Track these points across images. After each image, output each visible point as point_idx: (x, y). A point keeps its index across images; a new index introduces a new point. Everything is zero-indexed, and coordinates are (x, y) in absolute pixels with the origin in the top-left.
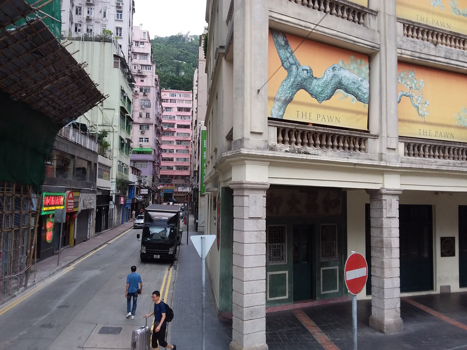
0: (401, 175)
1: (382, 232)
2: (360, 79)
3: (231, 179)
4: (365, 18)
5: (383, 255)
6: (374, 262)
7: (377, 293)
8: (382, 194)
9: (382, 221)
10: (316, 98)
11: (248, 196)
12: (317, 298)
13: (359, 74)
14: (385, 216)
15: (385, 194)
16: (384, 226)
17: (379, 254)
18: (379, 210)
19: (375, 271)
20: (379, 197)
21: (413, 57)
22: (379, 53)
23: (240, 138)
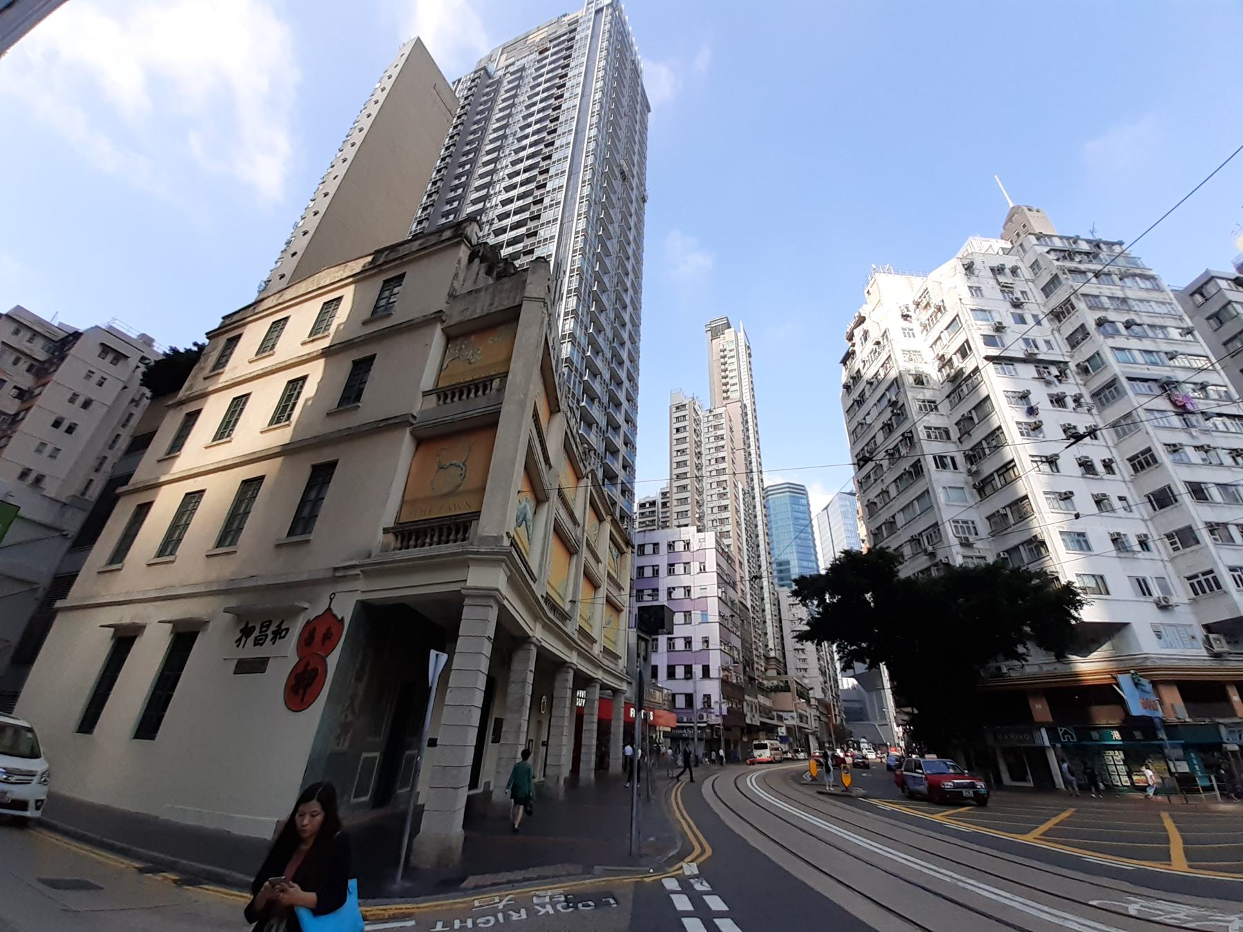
0: (543, 627)
11: (492, 607)
20: (526, 646)
23: (495, 535)
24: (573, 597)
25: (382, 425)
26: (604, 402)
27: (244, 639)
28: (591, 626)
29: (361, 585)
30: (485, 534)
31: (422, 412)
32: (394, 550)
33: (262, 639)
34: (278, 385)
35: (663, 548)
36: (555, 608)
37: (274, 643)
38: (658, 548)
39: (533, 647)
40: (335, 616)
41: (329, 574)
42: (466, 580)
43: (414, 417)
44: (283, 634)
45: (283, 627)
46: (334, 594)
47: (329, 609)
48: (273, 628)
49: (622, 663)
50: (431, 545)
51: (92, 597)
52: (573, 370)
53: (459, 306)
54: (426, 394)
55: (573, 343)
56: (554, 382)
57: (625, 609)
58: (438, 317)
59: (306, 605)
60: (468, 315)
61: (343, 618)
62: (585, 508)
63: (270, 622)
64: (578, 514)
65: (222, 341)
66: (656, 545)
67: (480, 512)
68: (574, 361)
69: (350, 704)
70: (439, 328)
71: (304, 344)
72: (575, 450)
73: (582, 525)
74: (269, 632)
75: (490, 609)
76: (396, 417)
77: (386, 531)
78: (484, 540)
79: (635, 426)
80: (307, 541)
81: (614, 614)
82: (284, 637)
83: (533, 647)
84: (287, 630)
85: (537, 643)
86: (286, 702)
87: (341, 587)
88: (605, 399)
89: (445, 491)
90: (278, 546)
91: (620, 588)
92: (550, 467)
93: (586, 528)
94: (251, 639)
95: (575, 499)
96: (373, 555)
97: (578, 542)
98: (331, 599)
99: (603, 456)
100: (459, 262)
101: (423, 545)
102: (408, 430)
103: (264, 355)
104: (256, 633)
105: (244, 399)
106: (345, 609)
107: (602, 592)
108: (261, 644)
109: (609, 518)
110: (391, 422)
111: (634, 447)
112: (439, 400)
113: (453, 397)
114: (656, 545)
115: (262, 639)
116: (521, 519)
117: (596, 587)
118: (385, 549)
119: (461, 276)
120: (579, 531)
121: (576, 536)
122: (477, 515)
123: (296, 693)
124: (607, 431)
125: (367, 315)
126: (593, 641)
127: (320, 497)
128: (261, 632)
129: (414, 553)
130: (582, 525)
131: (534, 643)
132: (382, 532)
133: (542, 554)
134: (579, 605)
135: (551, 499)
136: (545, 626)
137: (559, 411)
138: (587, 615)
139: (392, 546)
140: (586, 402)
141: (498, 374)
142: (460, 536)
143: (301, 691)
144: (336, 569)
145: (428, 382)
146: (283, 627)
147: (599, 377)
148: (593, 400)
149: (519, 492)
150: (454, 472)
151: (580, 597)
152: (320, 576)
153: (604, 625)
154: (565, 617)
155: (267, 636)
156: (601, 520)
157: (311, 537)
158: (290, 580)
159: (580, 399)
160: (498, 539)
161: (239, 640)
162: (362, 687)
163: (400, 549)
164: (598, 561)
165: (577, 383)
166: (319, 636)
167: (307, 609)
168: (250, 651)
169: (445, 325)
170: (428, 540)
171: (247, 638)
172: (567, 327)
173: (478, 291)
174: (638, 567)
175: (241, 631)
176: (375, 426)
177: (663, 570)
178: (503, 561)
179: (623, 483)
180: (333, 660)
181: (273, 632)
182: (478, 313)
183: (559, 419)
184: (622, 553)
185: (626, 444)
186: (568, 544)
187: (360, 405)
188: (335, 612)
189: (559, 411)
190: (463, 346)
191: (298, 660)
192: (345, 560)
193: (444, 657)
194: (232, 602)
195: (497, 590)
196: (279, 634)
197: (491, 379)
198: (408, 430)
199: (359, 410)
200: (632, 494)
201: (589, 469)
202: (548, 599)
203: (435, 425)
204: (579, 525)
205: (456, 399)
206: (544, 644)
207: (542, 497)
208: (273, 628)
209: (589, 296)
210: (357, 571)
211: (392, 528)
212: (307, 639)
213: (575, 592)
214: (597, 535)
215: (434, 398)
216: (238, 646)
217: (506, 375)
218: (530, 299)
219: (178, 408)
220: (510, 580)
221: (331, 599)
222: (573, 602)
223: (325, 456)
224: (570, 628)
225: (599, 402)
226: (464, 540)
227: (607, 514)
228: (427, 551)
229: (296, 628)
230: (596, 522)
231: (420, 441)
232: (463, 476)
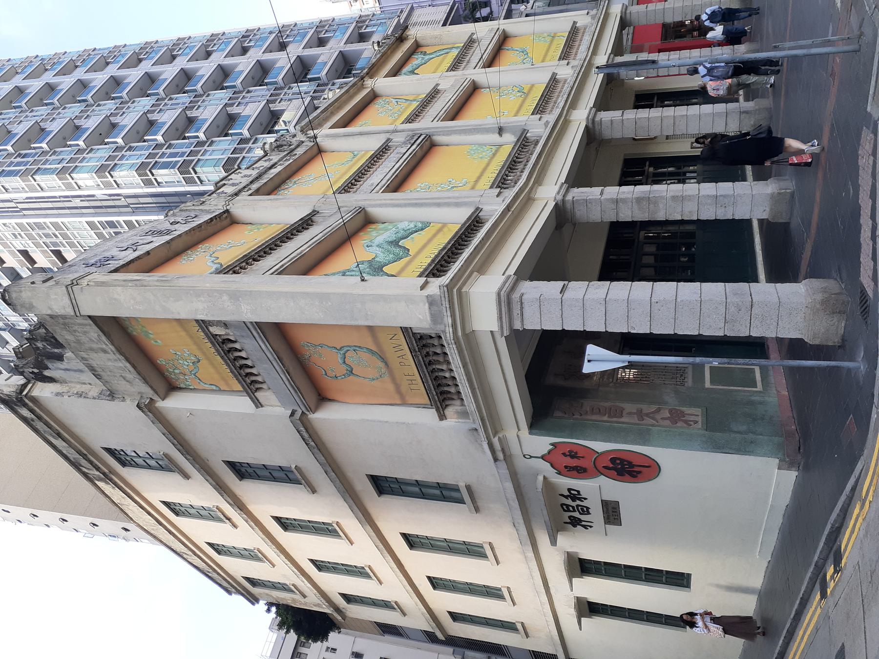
0: (540, 185)
1: (624, 201)
2: (394, 229)
4: (315, 221)
5: (662, 197)
6: (676, 214)
7: (727, 208)
8: (563, 201)
9: (608, 200)
10: (402, 258)
13: (386, 230)
15: (563, 196)
16: (615, 197)
17: (661, 206)
18: (589, 205)
19: (690, 212)
20: (569, 206)
21: (384, 185)
22: (366, 209)
23: (427, 305)
24: (493, 133)
25: (312, 443)
26: (188, 100)
27: (583, 523)
28: (533, 86)
29: (510, 433)
30: (429, 318)
31: (284, 405)
32: (464, 405)
33: (582, 509)
34: (290, 540)
36: (512, 165)
37: (585, 499)
39: (569, 197)
40: (549, 452)
41: (503, 465)
42: (492, 332)
43: (293, 414)
44: (576, 493)
45: (567, 493)
46: (524, 456)
47: (543, 457)
48: (569, 502)
49: (582, 17)
50: (451, 370)
51: (552, 638)
52: (153, 161)
53: (121, 386)
54: (258, 404)
55: (113, 169)
56: (186, 233)
57: (502, 28)
58: (148, 408)
59: (541, 478)
60: (131, 374)
61: (552, 444)
62: (361, 134)
63: (562, 505)
64: (374, 144)
65: (256, 591)
67: (401, 327)
68: (139, 161)
69: (650, 417)
70: (160, 404)
71: (235, 526)
72: (279, 168)
73: (388, 135)
74: (574, 504)
75: (523, 297)
76: (299, 432)
77: (442, 417)
78: (436, 318)
79: (213, 38)
80: (469, 488)
81: (511, 44)
82: (578, 492)
83: (569, 197)
84: (569, 490)
86: (649, 480)
87: (515, 449)
88: (184, 99)
89: (381, 364)
90: (477, 510)
91: (471, 42)
92: (315, 213)
93: (392, 127)
94: (583, 517)
95: (352, 152)
96: (474, 426)
97: (413, 137)
98: (531, 457)
99: (273, 87)
100: (58, 394)
101: (454, 378)
102: (311, 416)
103: (260, 555)
104: (576, 514)
105: (317, 563)
106: (542, 443)
107: (481, 75)
108: (588, 508)
109: (369, 83)
110: (306, 435)
111: (247, 35)
112: (261, 388)
113: (252, 374)
115: (582, 509)
116: (397, 250)
117: (474, 89)
118: (464, 414)
119: (78, 388)
120: (398, 139)
121: (405, 143)
122: (405, 331)
123: (640, 472)
124: (234, 87)
125: (176, 477)
126: (554, 82)
127: (415, 483)
128: (574, 511)
129: (465, 389)
130: (388, 135)
131: (564, 196)
132: (444, 423)
133: (439, 205)
134: (504, 121)
135: (362, 204)
136: (539, 182)
137: (227, 211)
138: (513, 100)
139: (459, 408)
140: (197, 131)
141: (204, 331)
142: (436, 342)
143: (636, 469)
144: (496, 460)
145: (242, 404)
146: (567, 493)
147: (151, 117)
148: (191, 121)
149: (363, 280)
150: (351, 358)
151: (490, 121)
152: (505, 471)
153: (529, 65)
154: (524, 143)
155: (578, 506)
156: (373, 96)
157: (462, 485)
158: (514, 496)
159: (195, 141)
160: (432, 302)
161: (585, 527)
162: (629, 407)
163: (462, 399)
164: (434, 94)
165: (172, 151)
166: (574, 463)
167: (545, 478)
168: (597, 515)
169: (155, 397)
170: (447, 375)
171: (580, 520)
172: (90, 183)
173: (92, 369)
175: (575, 526)
176: (316, 450)
178: (459, 290)
179: (308, 46)
181: (574, 500)
182: (124, 364)
183: (242, 208)
184: (417, 47)
185: (244, 51)
186: (419, 155)
187: (293, 467)
189: (227, 211)
190: (177, 371)
192: (484, 452)
194: (543, 539)
195: (499, 294)
196: (574, 495)
197: (213, 338)
198: (311, 416)
199: (300, 465)
200: (321, 25)
201: (301, 137)
202: (501, 183)
203: (298, 389)
204: (389, 140)
205: (254, 371)
206: (563, 179)
207: (360, 220)
208: (569, 502)
209: (25, 156)
210: (495, 441)
211: (438, 410)
212: (580, 472)
213: (486, 130)
214: (397, 99)
215: (258, 394)
216: (591, 527)
217: (204, 325)
218: (75, 306)
219: (344, 610)
220: (482, 268)
221: (531, 457)
222: (501, 131)
223: (367, 490)
224: (539, 128)
225: (192, 108)
226: (440, 337)
227: (363, 87)
228: (459, 373)
229: (566, 483)
230: (380, 101)
231: (322, 398)
232: (357, 348)
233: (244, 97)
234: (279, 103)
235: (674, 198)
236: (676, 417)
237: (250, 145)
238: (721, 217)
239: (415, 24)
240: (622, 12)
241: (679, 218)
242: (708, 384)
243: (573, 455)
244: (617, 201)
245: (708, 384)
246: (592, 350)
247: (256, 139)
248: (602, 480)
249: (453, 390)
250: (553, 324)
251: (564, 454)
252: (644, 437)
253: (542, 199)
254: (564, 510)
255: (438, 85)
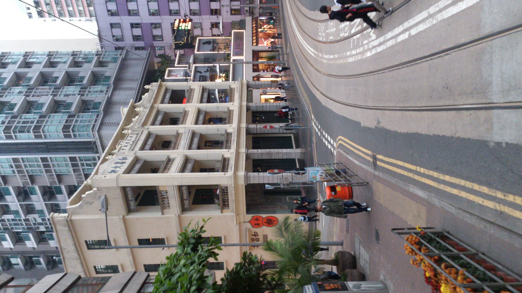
1: (264, 153)
3: (242, 185)
5: (273, 153)
12: (300, 189)
14: (257, 152)
17: (273, 155)
35: (115, 20)
38: (115, 24)
41: (238, 226)
44: (256, 233)
47: (249, 222)
48: (254, 237)
66: (112, 26)
82: (257, 233)
84: (255, 232)
85: (247, 151)
98: (246, 222)
106: (250, 217)
109: (156, 105)
114: (112, 26)
131: (248, 152)
146: (254, 234)
166: (256, 222)
174: (134, 40)
177: (135, 20)
180: (264, 216)
181: (255, 236)
188: (249, 220)
191: (264, 226)
193: (266, 186)
208: (254, 237)
215: (165, 211)
221: (246, 222)
233: (35, 92)
234: (59, 96)
235: (276, 153)
236: (281, 207)
237: (47, 119)
238: (288, 158)
239: (131, 59)
240: (247, 84)
241: (278, 158)
242: (288, 201)
243: (257, 219)
244: (262, 154)
245: (288, 201)
246: (266, 186)
247: (50, 116)
248: (264, 228)
249: (227, 203)
250: (256, 182)
251: (255, 220)
252: (274, 212)
253: (242, 153)
254: (252, 241)
255: (184, 109)
